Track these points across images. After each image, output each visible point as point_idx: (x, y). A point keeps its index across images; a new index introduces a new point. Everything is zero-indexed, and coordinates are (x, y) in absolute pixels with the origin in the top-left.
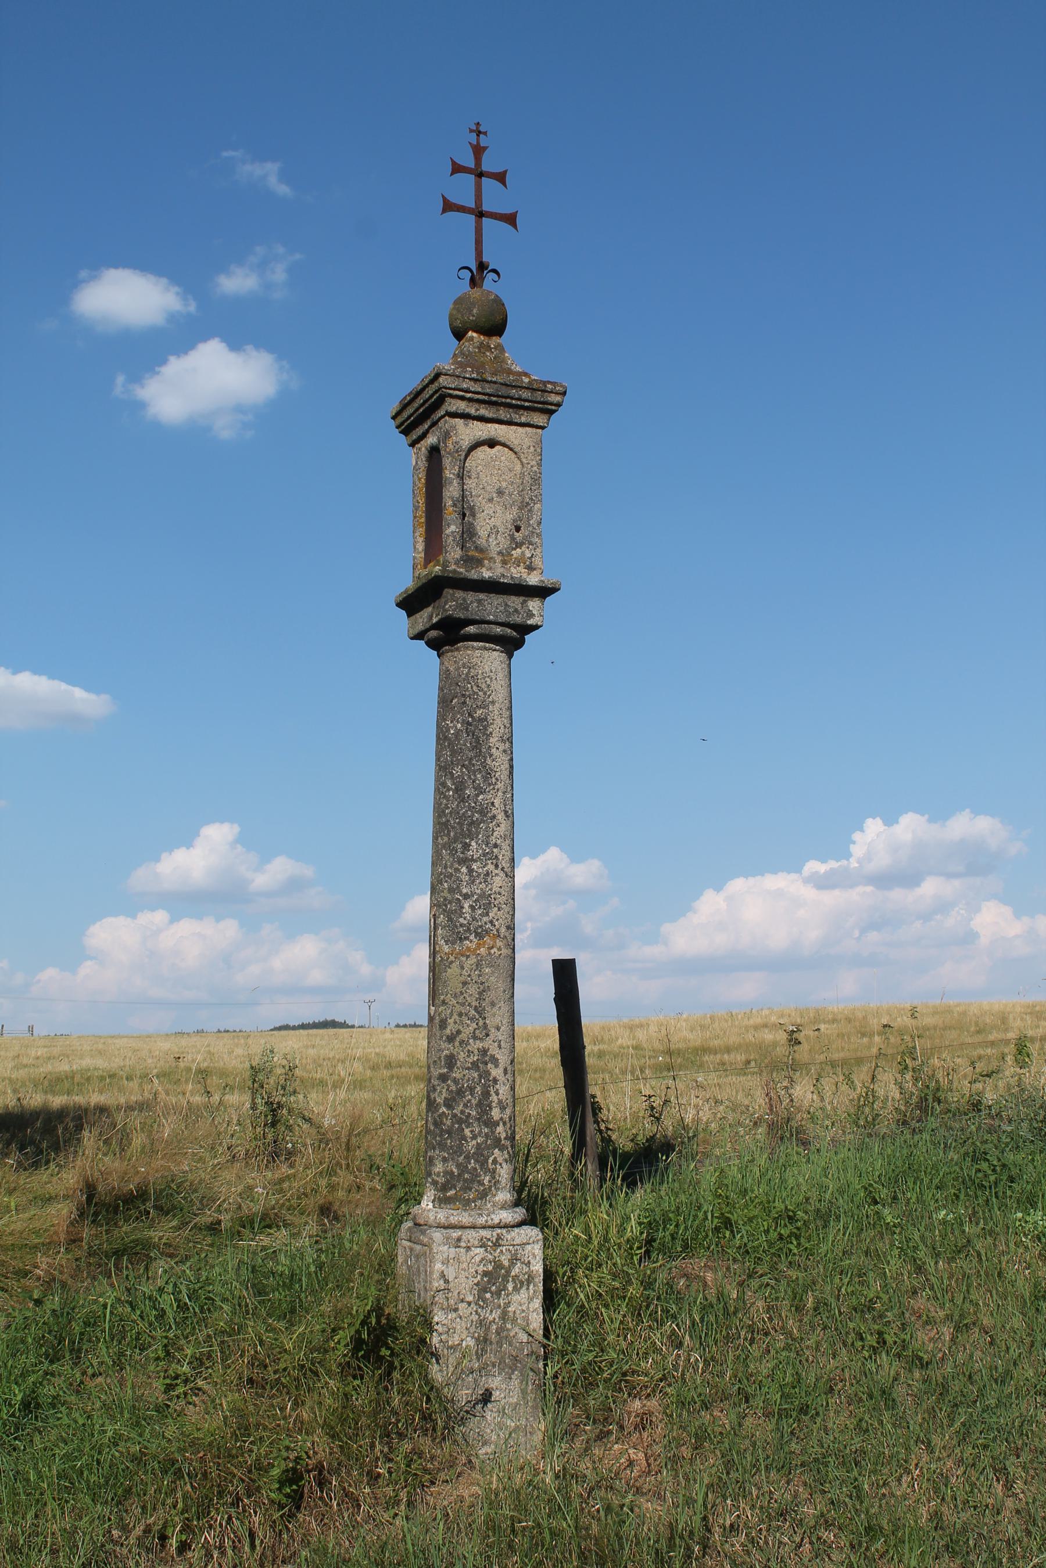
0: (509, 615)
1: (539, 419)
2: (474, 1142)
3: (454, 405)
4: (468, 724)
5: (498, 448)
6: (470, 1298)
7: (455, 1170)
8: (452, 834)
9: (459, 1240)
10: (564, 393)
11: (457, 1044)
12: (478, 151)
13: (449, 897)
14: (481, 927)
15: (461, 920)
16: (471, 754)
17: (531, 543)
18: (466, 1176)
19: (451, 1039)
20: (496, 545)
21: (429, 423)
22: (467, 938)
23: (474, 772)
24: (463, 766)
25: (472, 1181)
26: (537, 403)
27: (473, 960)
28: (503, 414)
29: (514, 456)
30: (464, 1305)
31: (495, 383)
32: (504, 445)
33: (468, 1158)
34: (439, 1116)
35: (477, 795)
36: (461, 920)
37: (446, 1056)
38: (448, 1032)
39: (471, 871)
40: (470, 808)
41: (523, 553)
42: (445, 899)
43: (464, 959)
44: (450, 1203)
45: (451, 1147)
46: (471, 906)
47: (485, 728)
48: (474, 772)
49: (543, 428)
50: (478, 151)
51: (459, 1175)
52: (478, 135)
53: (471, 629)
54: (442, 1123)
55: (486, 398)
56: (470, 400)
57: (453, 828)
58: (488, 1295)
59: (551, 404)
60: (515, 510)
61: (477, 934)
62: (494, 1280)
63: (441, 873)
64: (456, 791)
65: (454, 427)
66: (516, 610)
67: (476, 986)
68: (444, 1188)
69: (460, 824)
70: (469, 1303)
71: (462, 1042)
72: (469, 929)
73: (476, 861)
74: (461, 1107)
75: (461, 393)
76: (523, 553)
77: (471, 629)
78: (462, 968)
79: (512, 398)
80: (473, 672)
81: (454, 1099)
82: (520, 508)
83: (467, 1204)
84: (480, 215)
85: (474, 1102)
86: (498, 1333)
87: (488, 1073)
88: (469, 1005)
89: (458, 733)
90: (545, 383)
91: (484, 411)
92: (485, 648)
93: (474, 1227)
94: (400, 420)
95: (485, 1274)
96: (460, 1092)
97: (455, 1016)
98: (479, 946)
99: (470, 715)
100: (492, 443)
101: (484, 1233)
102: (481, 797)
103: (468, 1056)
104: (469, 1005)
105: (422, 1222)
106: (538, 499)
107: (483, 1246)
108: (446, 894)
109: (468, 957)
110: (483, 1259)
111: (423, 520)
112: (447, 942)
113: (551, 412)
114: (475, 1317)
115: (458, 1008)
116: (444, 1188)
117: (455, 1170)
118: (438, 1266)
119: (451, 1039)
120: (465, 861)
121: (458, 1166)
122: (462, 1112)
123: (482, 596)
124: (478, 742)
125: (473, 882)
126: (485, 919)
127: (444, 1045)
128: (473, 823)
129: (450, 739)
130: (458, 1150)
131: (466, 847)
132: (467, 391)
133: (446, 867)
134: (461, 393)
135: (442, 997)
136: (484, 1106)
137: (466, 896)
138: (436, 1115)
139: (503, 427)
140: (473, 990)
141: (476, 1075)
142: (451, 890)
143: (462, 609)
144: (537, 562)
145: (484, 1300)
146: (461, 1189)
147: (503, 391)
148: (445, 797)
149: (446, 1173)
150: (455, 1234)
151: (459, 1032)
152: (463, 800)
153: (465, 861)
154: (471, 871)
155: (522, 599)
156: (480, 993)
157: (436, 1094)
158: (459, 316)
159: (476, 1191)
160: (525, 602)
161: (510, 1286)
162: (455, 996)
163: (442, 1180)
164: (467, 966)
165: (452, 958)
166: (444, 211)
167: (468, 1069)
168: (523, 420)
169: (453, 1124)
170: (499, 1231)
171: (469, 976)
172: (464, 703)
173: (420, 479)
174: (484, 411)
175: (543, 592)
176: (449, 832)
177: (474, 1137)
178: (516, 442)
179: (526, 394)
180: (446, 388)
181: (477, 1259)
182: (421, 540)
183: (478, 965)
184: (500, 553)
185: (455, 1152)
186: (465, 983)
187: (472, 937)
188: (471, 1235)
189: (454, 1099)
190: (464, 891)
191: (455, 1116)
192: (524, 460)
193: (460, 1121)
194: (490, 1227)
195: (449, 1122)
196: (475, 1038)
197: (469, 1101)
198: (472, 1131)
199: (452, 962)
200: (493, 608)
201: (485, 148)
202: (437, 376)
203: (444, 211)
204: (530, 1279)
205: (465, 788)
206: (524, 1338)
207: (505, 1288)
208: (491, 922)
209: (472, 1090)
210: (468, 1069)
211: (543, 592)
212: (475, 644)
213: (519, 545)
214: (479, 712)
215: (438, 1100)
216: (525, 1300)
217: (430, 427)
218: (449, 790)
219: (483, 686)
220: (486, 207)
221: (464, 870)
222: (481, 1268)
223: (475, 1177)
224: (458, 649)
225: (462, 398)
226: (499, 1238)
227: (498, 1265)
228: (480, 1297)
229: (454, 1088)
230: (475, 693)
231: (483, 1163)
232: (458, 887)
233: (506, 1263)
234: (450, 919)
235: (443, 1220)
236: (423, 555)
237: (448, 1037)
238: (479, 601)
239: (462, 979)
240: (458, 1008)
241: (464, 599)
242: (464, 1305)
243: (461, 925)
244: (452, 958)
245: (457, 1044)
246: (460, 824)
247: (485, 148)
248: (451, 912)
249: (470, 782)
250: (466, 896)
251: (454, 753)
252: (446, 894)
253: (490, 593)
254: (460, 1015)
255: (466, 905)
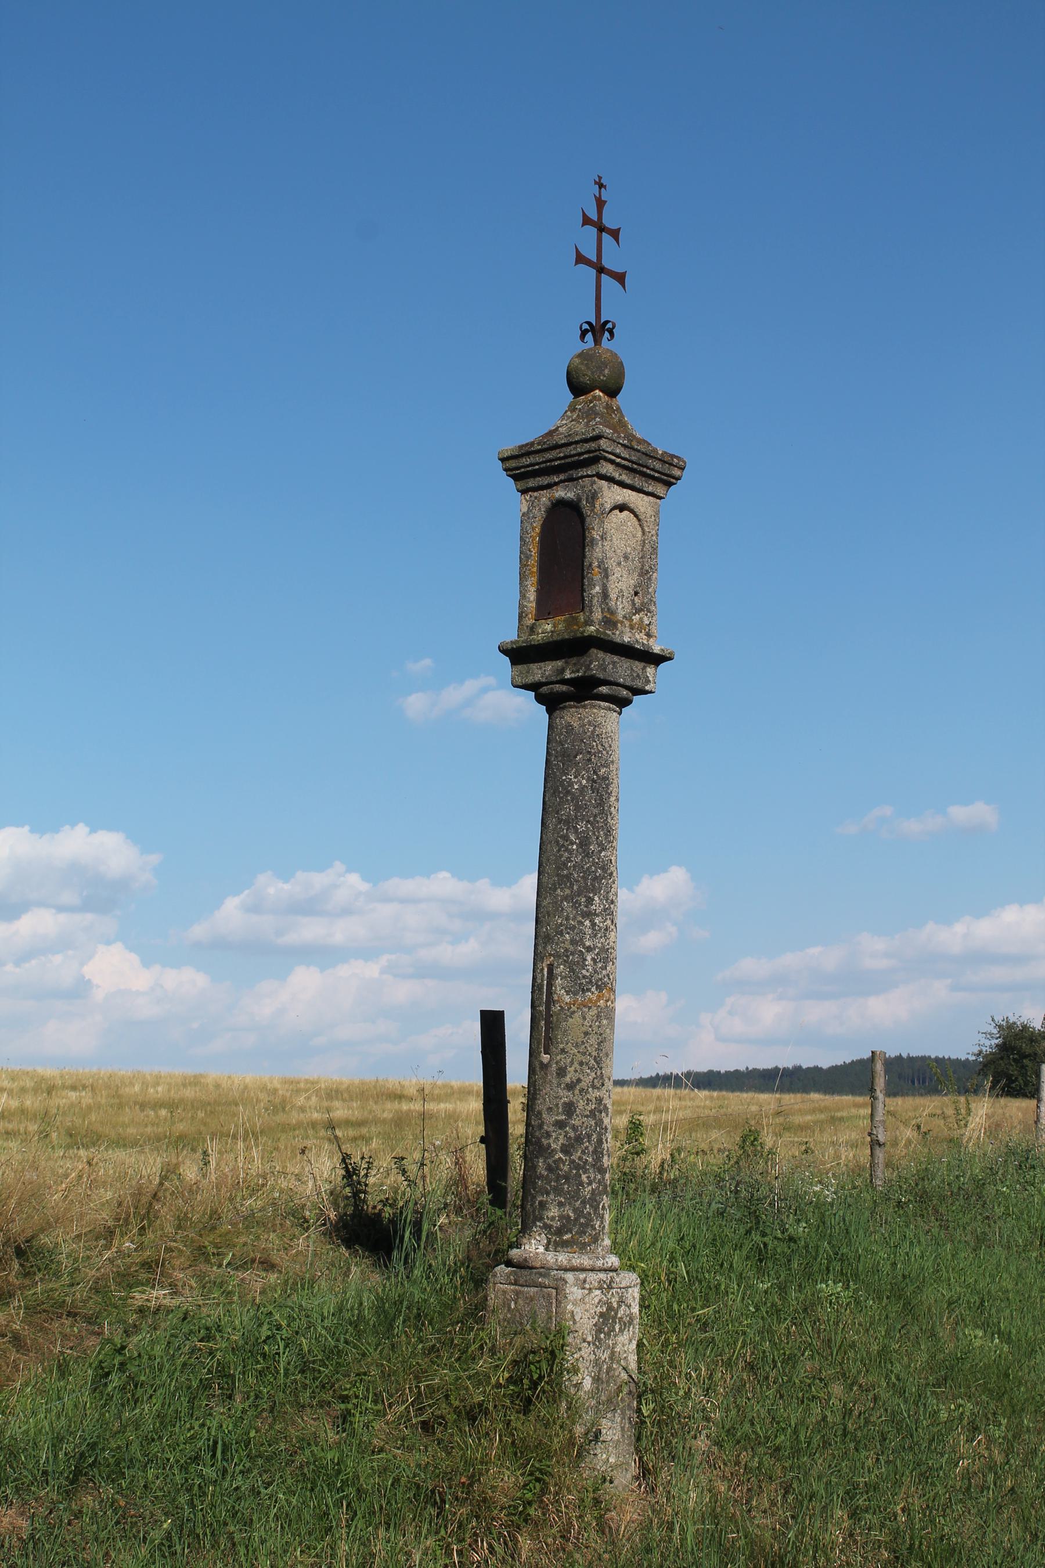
0: (633, 680)
1: (660, 490)
2: (590, 1188)
3: (607, 469)
4: (594, 781)
5: (626, 513)
6: (590, 1339)
7: (571, 1215)
8: (575, 887)
9: (585, 1281)
10: (683, 469)
11: (577, 1092)
12: (600, 204)
13: (571, 948)
14: (601, 979)
15: (584, 972)
16: (595, 811)
17: (649, 611)
18: (582, 1220)
19: (570, 1087)
20: (622, 608)
21: (562, 477)
22: (589, 990)
23: (598, 828)
24: (588, 822)
25: (587, 1225)
26: (655, 472)
27: (594, 1012)
28: (638, 481)
29: (637, 523)
30: (585, 1344)
31: (639, 451)
32: (632, 511)
33: (584, 1203)
34: (554, 1162)
35: (600, 852)
36: (584, 972)
37: (565, 1103)
38: (568, 1079)
39: (593, 924)
40: (594, 864)
41: (641, 619)
42: (566, 950)
43: (586, 1010)
44: (567, 1247)
45: (569, 1192)
46: (593, 959)
47: (608, 786)
48: (598, 828)
49: (660, 498)
50: (600, 204)
51: (576, 1219)
52: (600, 188)
53: (604, 690)
54: (558, 1168)
55: (630, 464)
56: (618, 465)
57: (577, 881)
58: (602, 1336)
59: (674, 478)
60: (636, 575)
61: (598, 987)
62: (608, 1320)
63: (561, 925)
64: (580, 845)
65: (600, 488)
66: (638, 675)
67: (595, 1037)
68: (559, 1232)
69: (585, 878)
70: (589, 1343)
71: (581, 1090)
72: (591, 981)
73: (598, 916)
74: (579, 1154)
75: (613, 458)
76: (641, 619)
77: (604, 690)
78: (584, 1018)
79: (648, 468)
80: (598, 731)
81: (573, 1146)
82: (641, 575)
83: (583, 1247)
84: (601, 270)
85: (591, 1149)
86: (608, 1373)
87: (601, 1121)
88: (590, 1054)
89: (582, 788)
90: (673, 456)
91: (625, 478)
92: (610, 709)
93: (592, 1270)
94: (513, 464)
95: (602, 1315)
96: (579, 1139)
97: (576, 1065)
98: (599, 998)
99: (595, 772)
100: (622, 508)
101: (602, 1276)
102: (603, 854)
103: (587, 1104)
104: (590, 1054)
105: (538, 1265)
106: (653, 568)
107: (600, 1288)
108: (567, 945)
109: (590, 1008)
110: (600, 1301)
111: (535, 569)
112: (568, 993)
113: (669, 484)
114: (592, 1357)
115: (580, 1057)
116: (559, 1232)
117: (571, 1215)
118: (570, 1307)
119: (570, 1087)
120: (589, 915)
121: (575, 1211)
122: (580, 1158)
123: (616, 658)
124: (601, 799)
125: (595, 936)
126: (604, 972)
127: (561, 1093)
128: (595, 878)
129: (573, 794)
130: (576, 1195)
131: (590, 901)
132: (618, 456)
133: (567, 919)
134: (613, 458)
135: (561, 1046)
136: (598, 1153)
137: (589, 949)
138: (550, 1161)
139: (634, 493)
140: (593, 1040)
141: (593, 1123)
142: (573, 942)
143: (576, 663)
144: (654, 630)
145: (600, 1340)
146: (577, 1233)
147: (644, 460)
148: (567, 850)
149: (561, 1217)
150: (582, 1276)
151: (579, 1081)
152: (587, 855)
153: (589, 915)
154: (593, 924)
155: (643, 664)
156: (599, 1044)
157: (551, 1141)
158: (589, 373)
159: (590, 1235)
160: (644, 668)
161: (617, 1327)
162: (577, 1046)
163: (557, 1224)
164: (588, 1017)
165: (574, 1008)
166: (577, 263)
167: (587, 1116)
168: (650, 489)
169: (571, 1169)
170: (611, 1274)
171: (590, 1026)
172: (590, 760)
173: (533, 529)
174: (625, 478)
175: (657, 660)
176: (572, 885)
177: (590, 1183)
178: (642, 510)
179: (658, 466)
180: (604, 451)
181: (596, 1300)
182: (533, 589)
183: (598, 1016)
184: (624, 617)
185: (573, 1197)
186: (586, 1034)
187: (593, 989)
188: (593, 1278)
189: (573, 1146)
190: (588, 944)
191: (573, 1162)
192: (646, 529)
193: (578, 1167)
194: (605, 1270)
195: (566, 1168)
196: (594, 1087)
197: (587, 1148)
198: (588, 1177)
199: (574, 1012)
200: (622, 670)
201: (605, 202)
202: (599, 437)
203: (577, 263)
204: (631, 1317)
205: (590, 844)
206: (624, 1376)
207: (614, 1330)
208: (608, 975)
209: (589, 1136)
210: (587, 1116)
211: (657, 660)
212: (602, 704)
213: (638, 611)
214: (603, 770)
215: (554, 1146)
216: (627, 1342)
217: (562, 481)
218: (572, 843)
219: (606, 745)
220: (606, 263)
221: (587, 923)
222: (599, 1310)
223: (589, 1224)
224: (585, 707)
225: (612, 462)
226: (612, 1281)
227: (610, 1308)
228: (598, 1338)
229: (572, 1135)
230: (600, 752)
231: (596, 1209)
232: (581, 939)
233: (615, 1305)
234: (572, 970)
235: (565, 1262)
236: (534, 605)
237: (567, 1085)
238: (614, 663)
239: (584, 1029)
240: (580, 1057)
241: (604, 660)
242: (585, 1344)
243: (584, 977)
244: (574, 1008)
245: (577, 1092)
246: (585, 878)
247: (605, 202)
248: (573, 963)
249: (594, 838)
250: (589, 949)
251: (578, 808)
252: (567, 945)
253: (622, 656)
254: (581, 1064)
255: (589, 958)
